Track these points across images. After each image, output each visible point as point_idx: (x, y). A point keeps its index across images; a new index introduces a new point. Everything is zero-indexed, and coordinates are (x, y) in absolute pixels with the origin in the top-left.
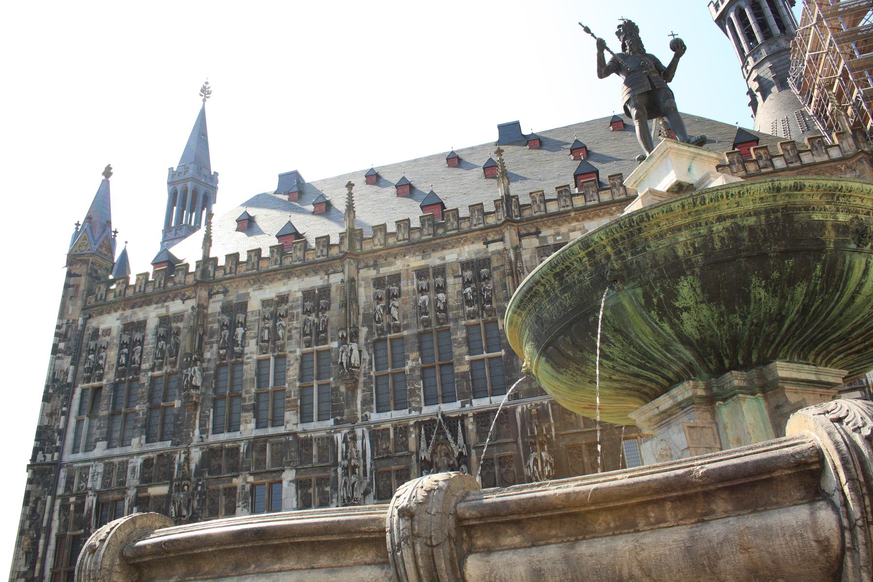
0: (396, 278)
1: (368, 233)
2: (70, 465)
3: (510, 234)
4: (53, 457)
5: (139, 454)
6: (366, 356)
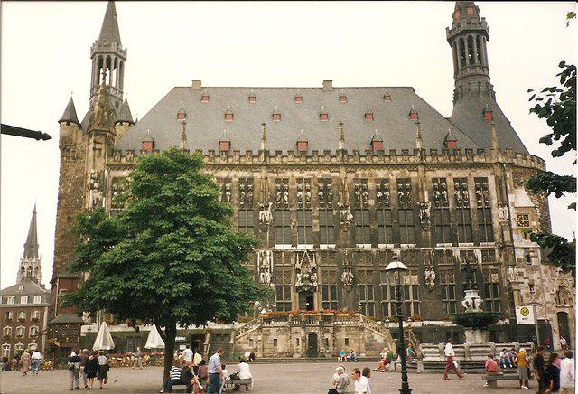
0: (286, 180)
1: (272, 153)
3: (343, 170)
6: (271, 217)
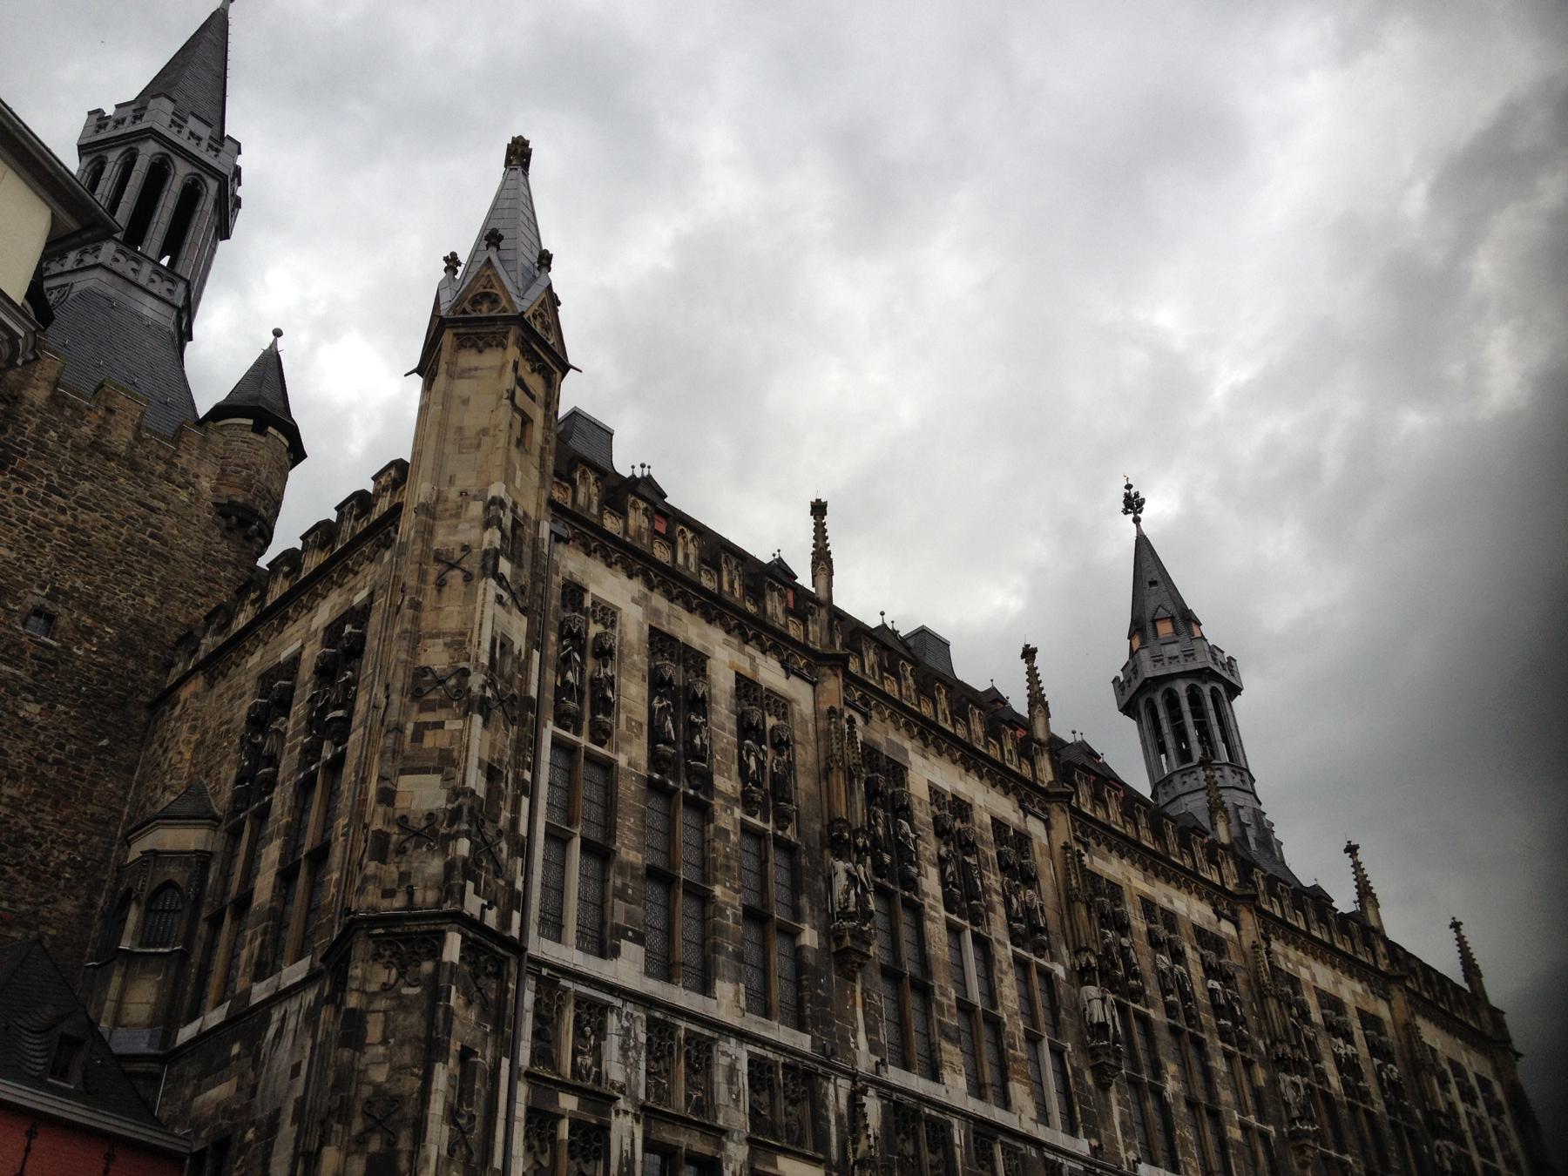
2: (551, 978)
4: (505, 921)
5: (743, 1036)
